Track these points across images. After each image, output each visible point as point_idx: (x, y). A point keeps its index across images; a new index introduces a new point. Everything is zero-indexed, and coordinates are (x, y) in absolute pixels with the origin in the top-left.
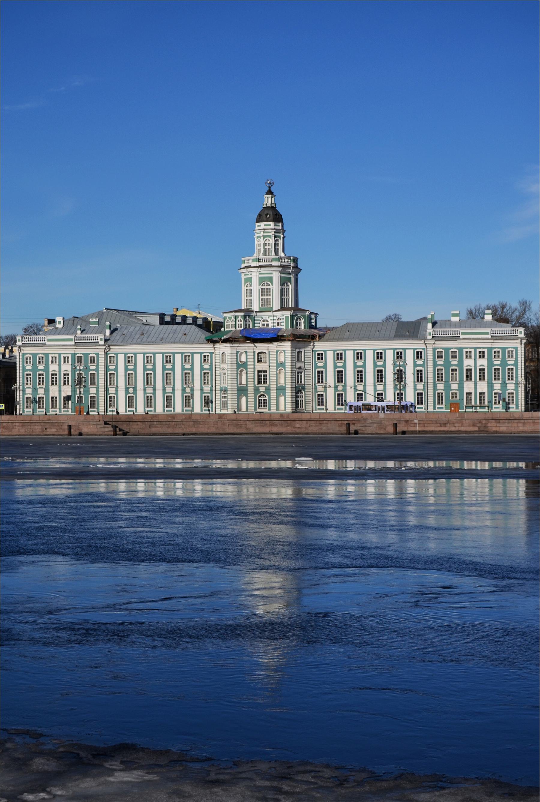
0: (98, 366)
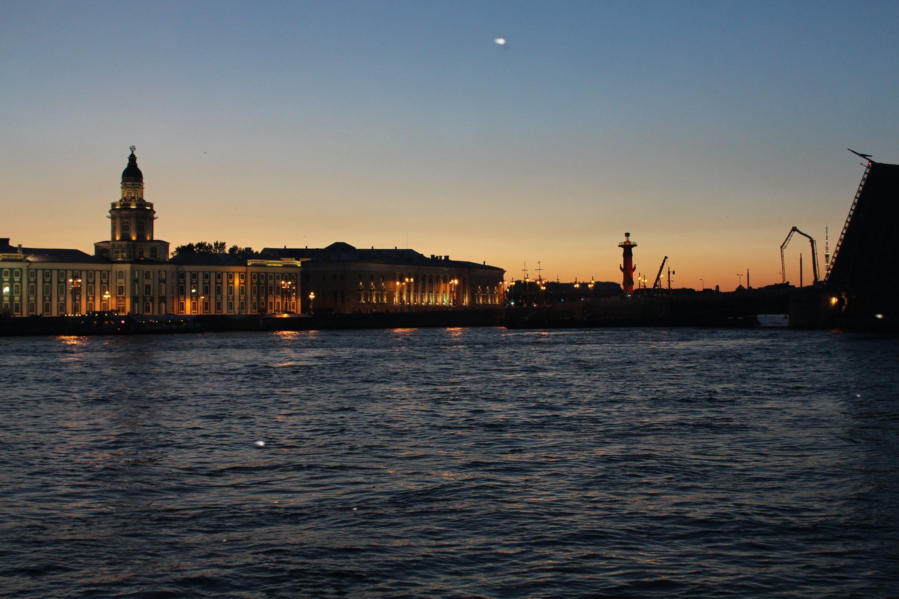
0: (21, 279)
